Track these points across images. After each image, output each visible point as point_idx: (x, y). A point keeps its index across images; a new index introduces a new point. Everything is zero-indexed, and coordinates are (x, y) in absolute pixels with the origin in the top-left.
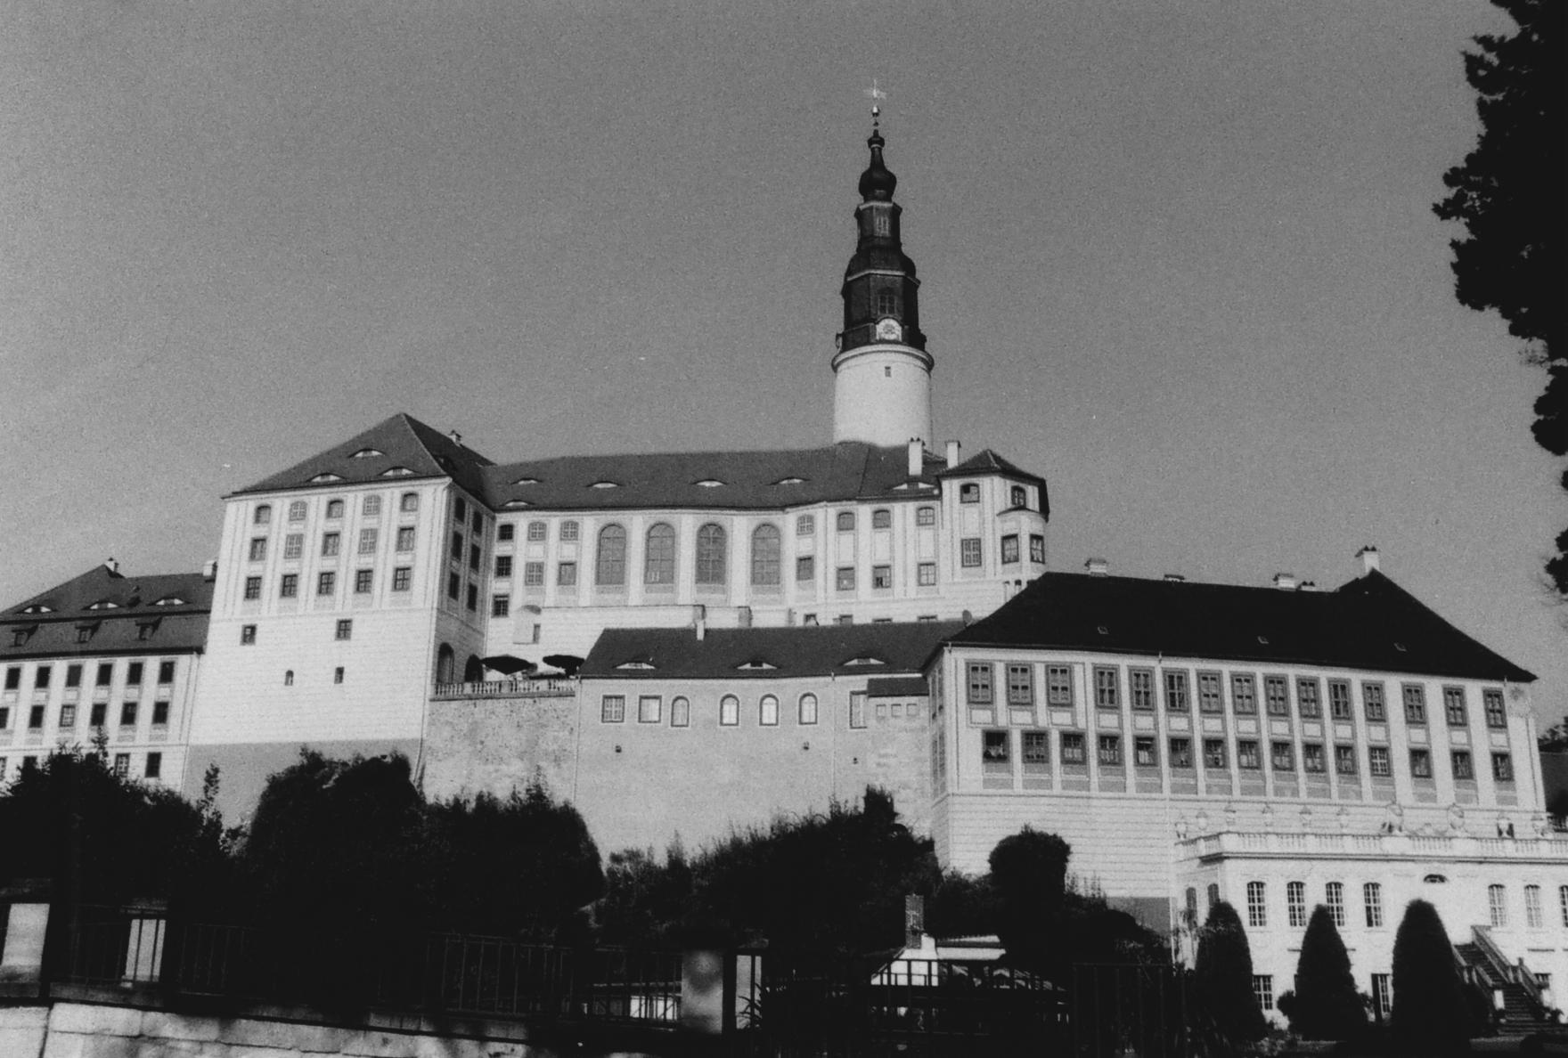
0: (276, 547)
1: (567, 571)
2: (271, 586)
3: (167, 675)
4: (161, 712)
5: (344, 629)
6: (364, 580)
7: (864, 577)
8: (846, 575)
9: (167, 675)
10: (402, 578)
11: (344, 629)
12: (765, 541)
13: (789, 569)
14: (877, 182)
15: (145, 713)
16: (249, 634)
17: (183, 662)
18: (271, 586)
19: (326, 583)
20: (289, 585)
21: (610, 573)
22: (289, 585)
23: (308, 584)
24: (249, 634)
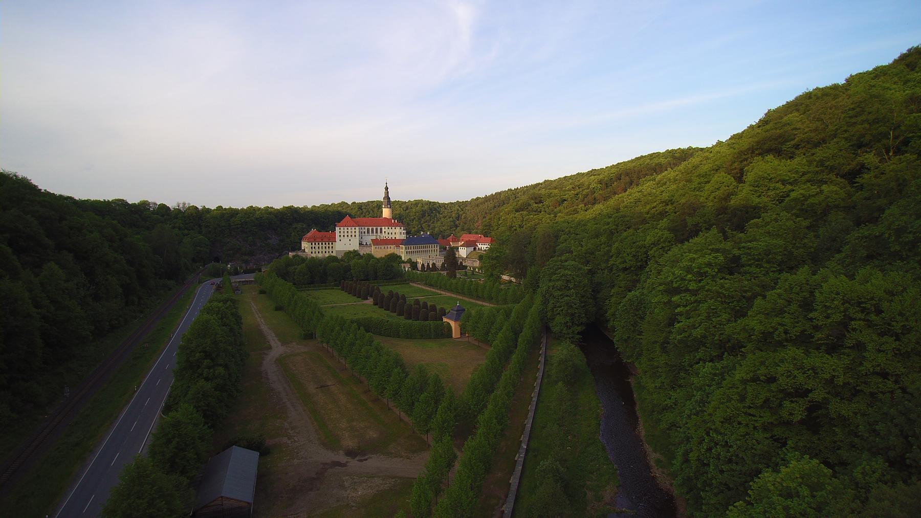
0: (342, 232)
1: (364, 232)
2: (342, 236)
3: (332, 244)
4: (332, 247)
5: (350, 240)
6: (351, 236)
7: (390, 233)
8: (388, 233)
9: (332, 244)
10: (355, 236)
11: (350, 240)
12: (381, 229)
13: (383, 232)
14: (387, 189)
15: (330, 247)
16: (340, 240)
17: (334, 243)
18: (342, 236)
19: (348, 236)
20: (344, 236)
21: (368, 232)
22: (344, 236)
23: (346, 236)
24: (340, 240)
